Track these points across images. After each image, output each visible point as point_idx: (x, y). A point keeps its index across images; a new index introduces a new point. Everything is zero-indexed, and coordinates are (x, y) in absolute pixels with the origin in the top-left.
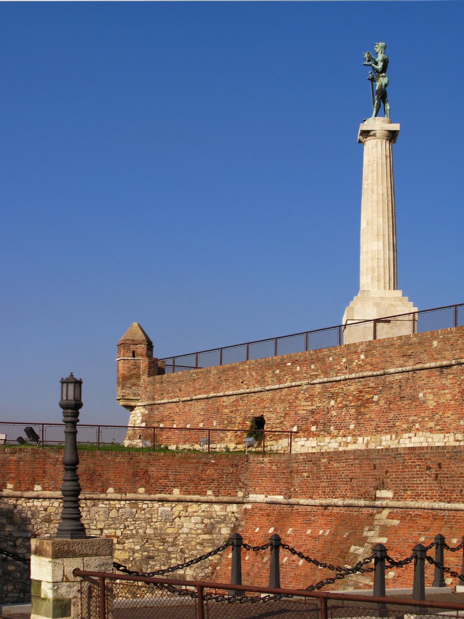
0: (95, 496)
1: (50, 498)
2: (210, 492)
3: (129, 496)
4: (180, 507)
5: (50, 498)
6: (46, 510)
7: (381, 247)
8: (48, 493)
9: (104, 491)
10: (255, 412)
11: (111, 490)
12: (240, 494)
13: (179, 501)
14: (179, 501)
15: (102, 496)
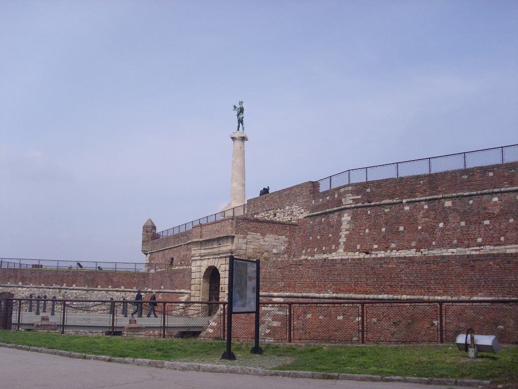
0: (93, 289)
1: (78, 290)
2: (134, 288)
3: (105, 289)
4: (123, 293)
5: (78, 290)
6: (76, 294)
7: (237, 185)
8: (77, 288)
9: (97, 287)
10: (172, 256)
11: (99, 286)
12: (146, 288)
13: (123, 291)
14: (123, 291)
15: (96, 289)
